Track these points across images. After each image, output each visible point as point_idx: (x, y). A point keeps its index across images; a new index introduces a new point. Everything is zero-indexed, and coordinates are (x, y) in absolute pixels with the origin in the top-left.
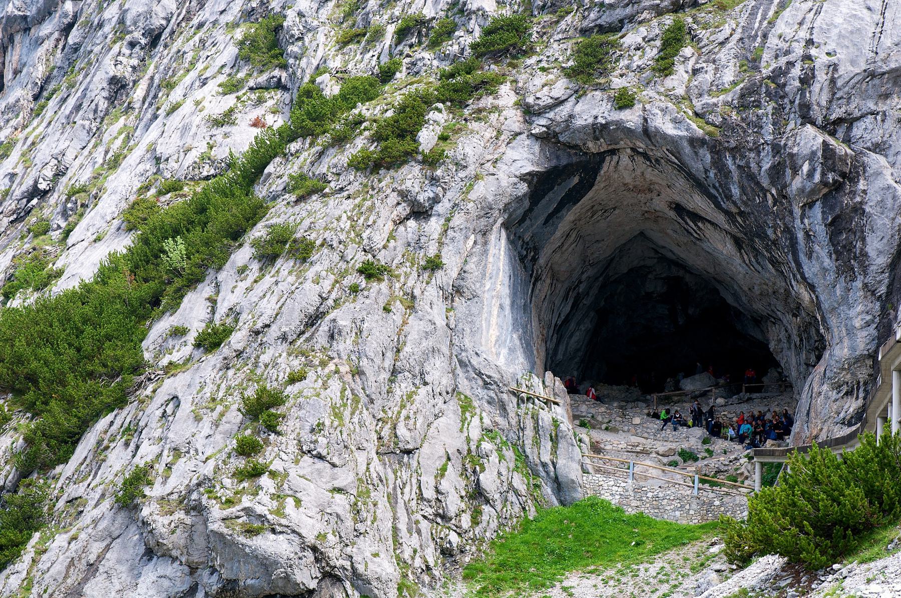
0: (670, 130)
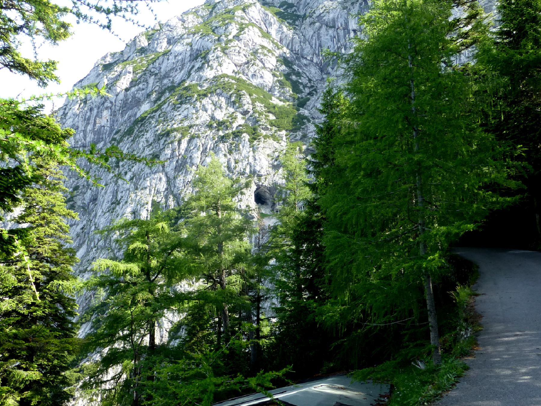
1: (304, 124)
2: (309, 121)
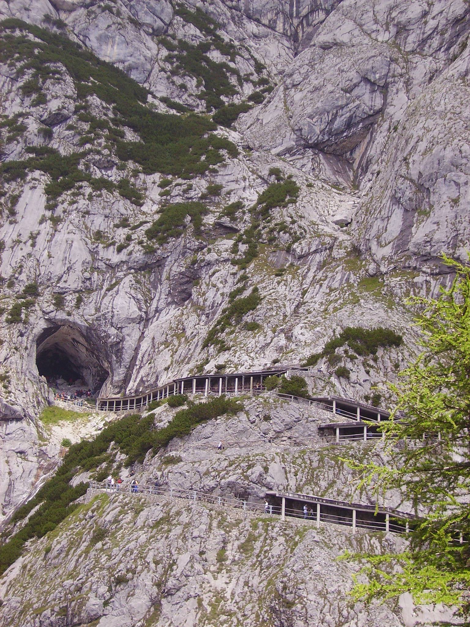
0: (79, 322)
1: (219, 159)
2: (234, 153)
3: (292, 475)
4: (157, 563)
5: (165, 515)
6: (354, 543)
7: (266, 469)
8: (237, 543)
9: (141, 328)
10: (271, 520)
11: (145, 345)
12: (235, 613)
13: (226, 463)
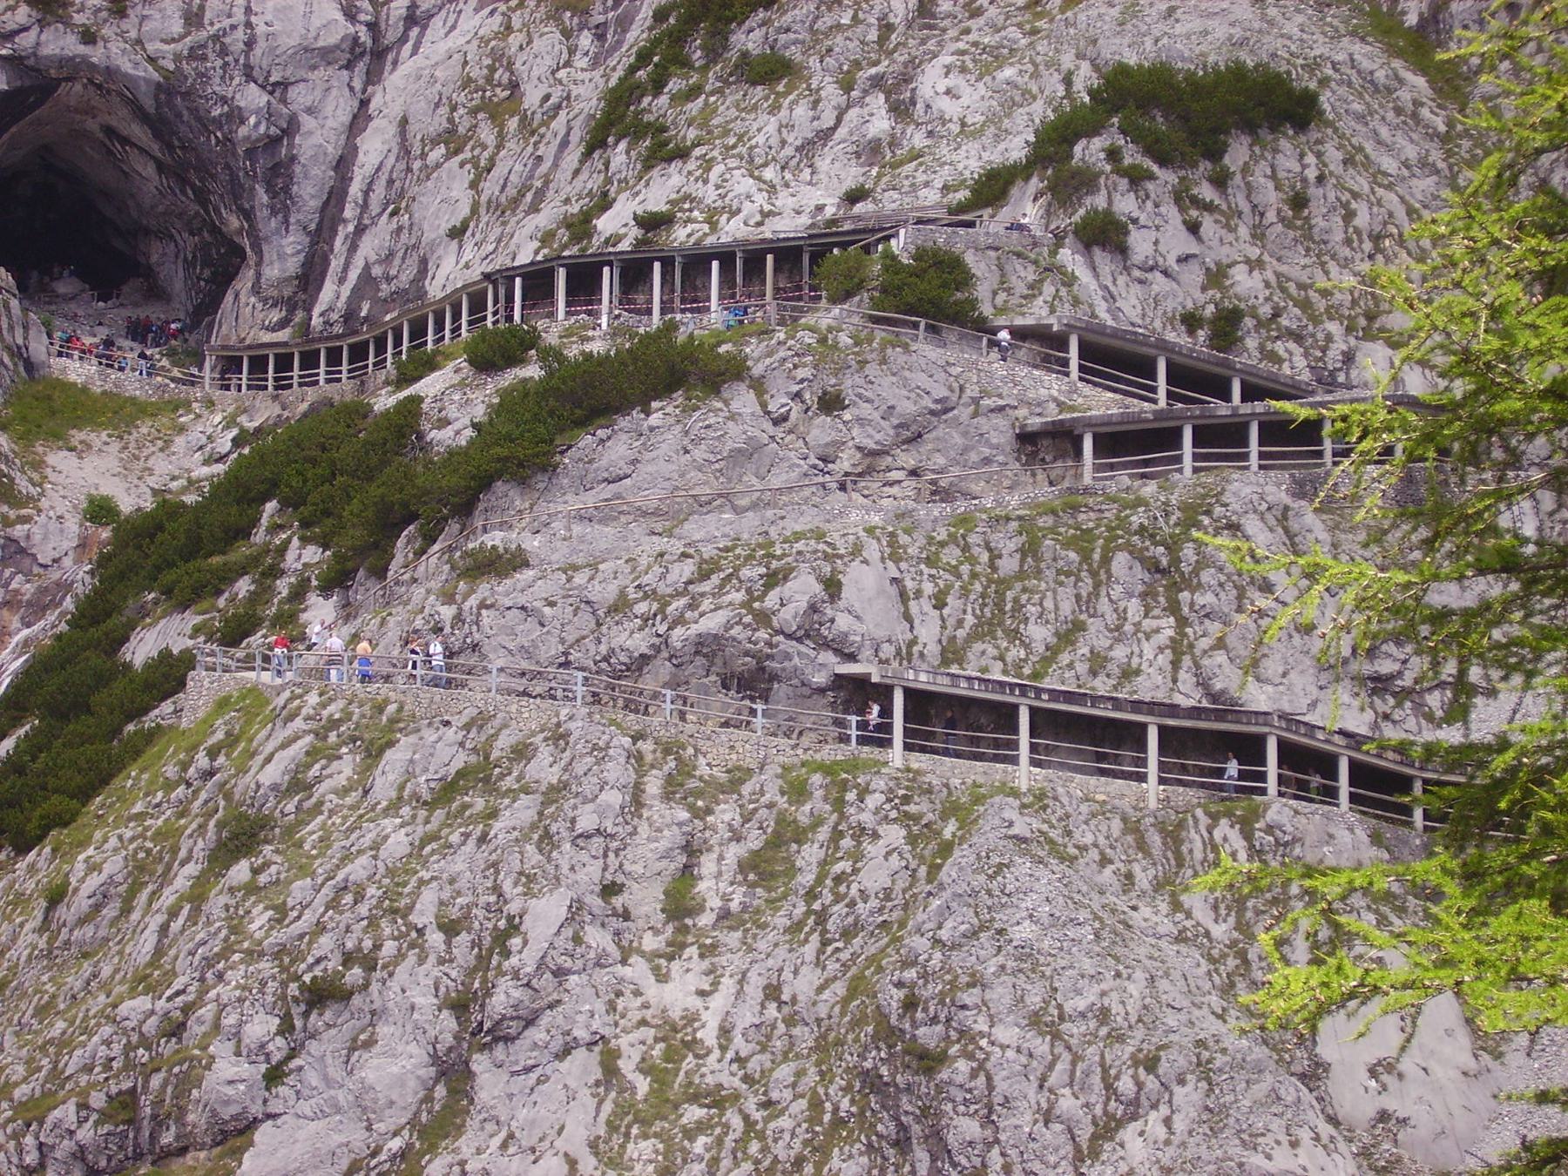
0: (126, 67)
3: (927, 606)
4: (450, 929)
5: (473, 759)
6: (1155, 839)
7: (833, 587)
8: (734, 852)
9: (358, 84)
10: (854, 766)
11: (374, 147)
12: (736, 1097)
13: (688, 569)
